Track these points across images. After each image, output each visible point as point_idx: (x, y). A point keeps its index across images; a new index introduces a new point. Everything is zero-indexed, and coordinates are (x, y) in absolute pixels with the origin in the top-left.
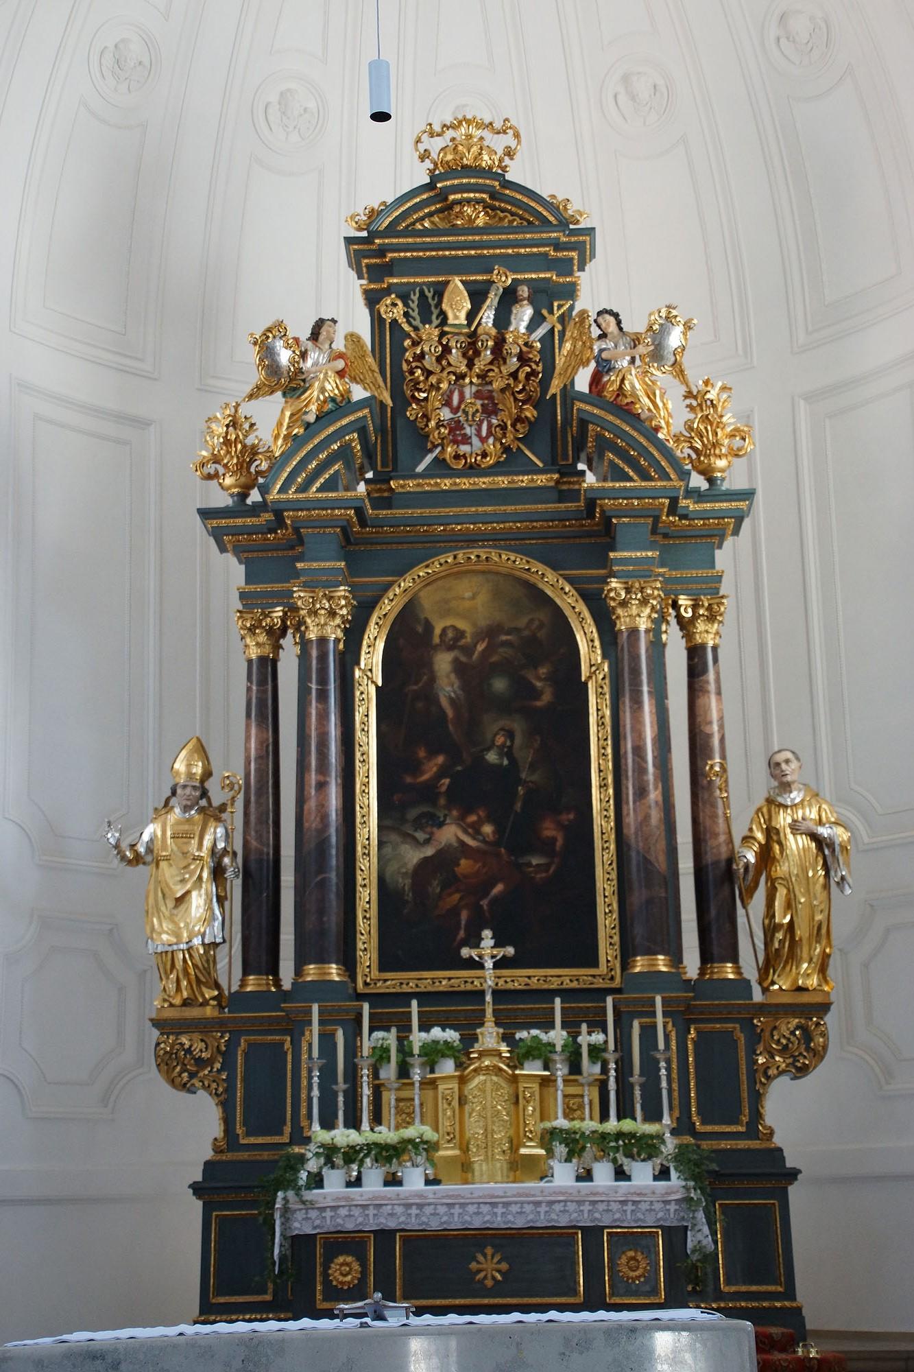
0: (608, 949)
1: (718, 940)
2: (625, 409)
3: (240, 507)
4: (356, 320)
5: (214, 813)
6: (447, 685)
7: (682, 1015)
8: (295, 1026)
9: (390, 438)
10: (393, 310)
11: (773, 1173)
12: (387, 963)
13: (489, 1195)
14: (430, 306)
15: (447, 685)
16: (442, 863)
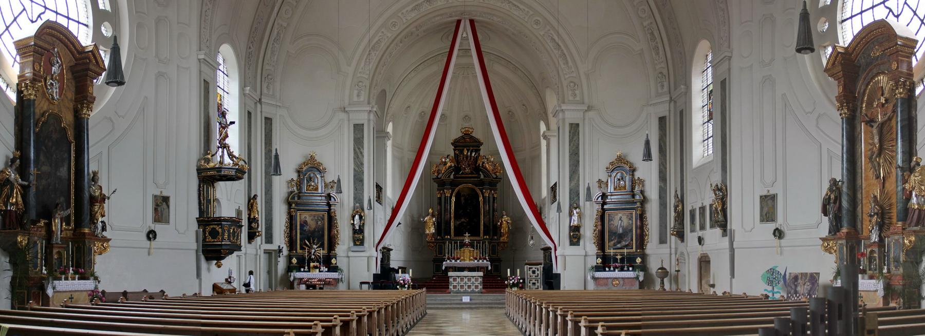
0: (482, 235)
1: (495, 234)
2: (485, 168)
3: (437, 178)
4: (452, 154)
5: (433, 216)
6: (463, 201)
7: (489, 243)
8: (445, 243)
9: (457, 169)
10: (457, 152)
11: (499, 260)
12: (455, 235)
13: (467, 263)
14: (462, 152)
15: (463, 201)
16: (461, 224)
